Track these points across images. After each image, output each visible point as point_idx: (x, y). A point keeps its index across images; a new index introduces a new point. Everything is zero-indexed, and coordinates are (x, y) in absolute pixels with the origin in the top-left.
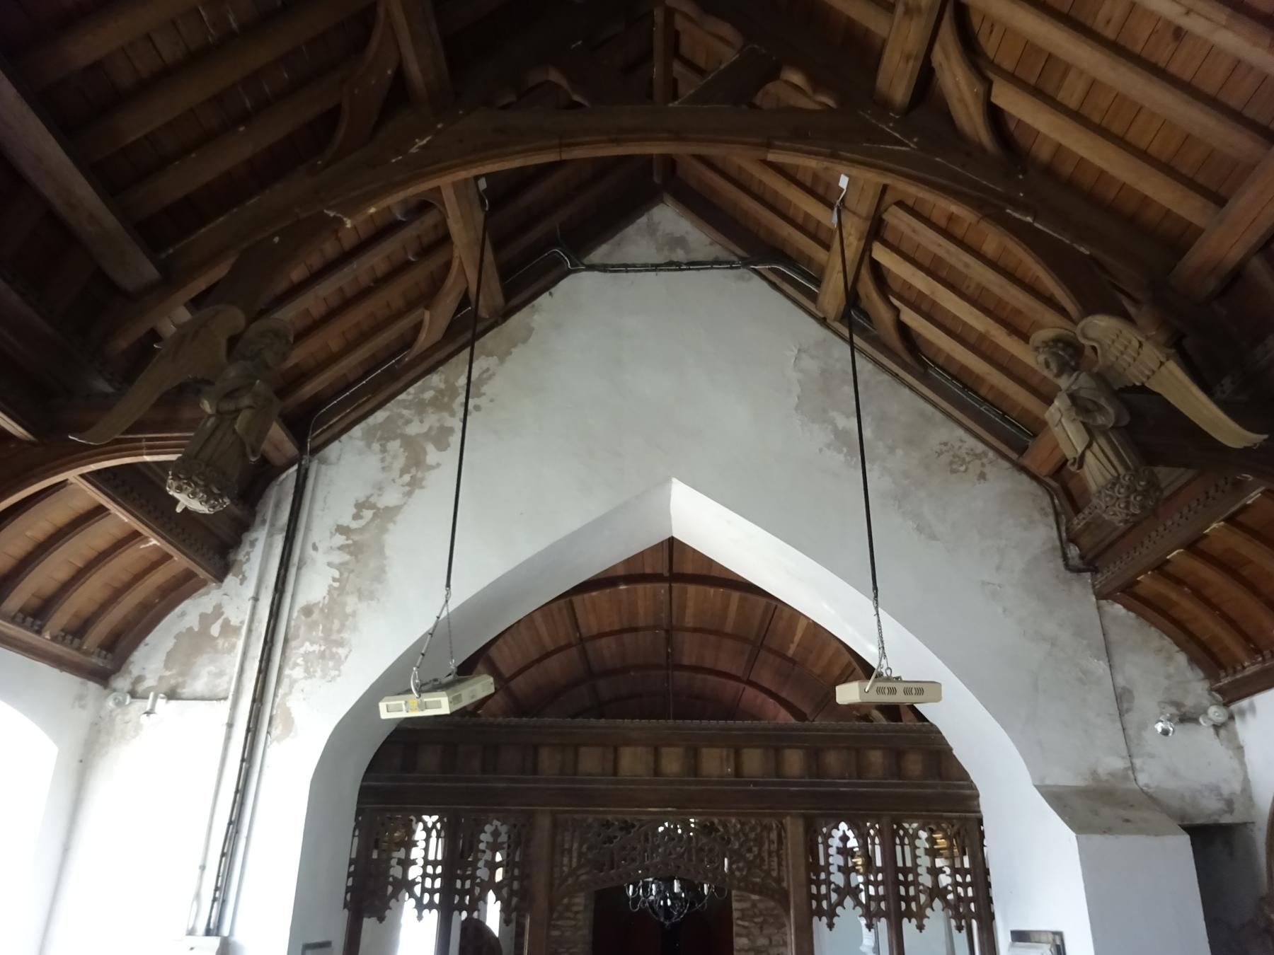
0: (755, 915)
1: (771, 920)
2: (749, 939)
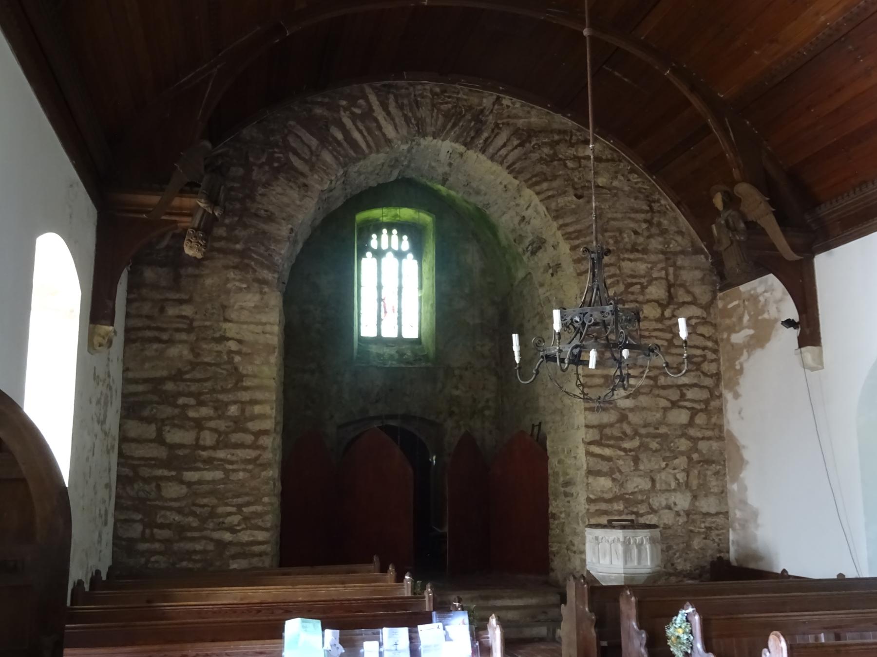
1: (654, 445)
2: (614, 480)
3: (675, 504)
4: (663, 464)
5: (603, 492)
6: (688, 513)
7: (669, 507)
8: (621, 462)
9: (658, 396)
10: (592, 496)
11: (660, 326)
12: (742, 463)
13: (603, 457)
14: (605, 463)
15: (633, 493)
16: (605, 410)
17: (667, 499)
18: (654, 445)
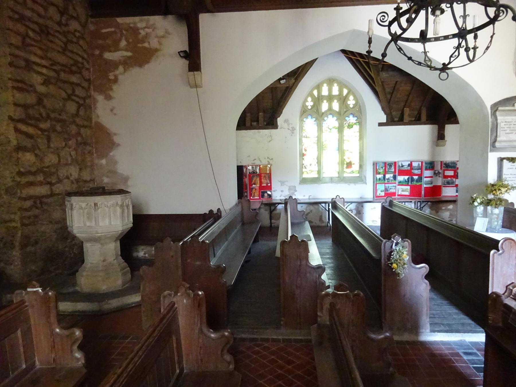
0: (41, 118)
2: (36, 155)
3: (71, 175)
4: (64, 144)
5: (30, 166)
6: (78, 181)
7: (68, 178)
8: (39, 140)
9: (60, 88)
10: (22, 170)
11: (58, 29)
12: (113, 145)
13: (30, 136)
14: (29, 140)
15: (48, 167)
16: (28, 91)
17: (67, 171)
18: (58, 128)
